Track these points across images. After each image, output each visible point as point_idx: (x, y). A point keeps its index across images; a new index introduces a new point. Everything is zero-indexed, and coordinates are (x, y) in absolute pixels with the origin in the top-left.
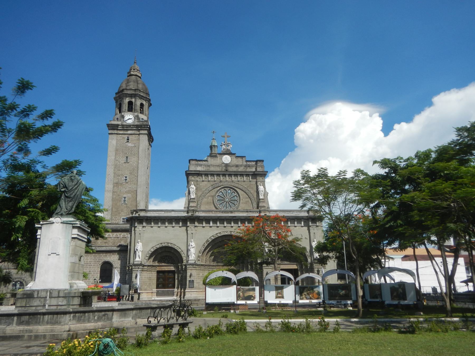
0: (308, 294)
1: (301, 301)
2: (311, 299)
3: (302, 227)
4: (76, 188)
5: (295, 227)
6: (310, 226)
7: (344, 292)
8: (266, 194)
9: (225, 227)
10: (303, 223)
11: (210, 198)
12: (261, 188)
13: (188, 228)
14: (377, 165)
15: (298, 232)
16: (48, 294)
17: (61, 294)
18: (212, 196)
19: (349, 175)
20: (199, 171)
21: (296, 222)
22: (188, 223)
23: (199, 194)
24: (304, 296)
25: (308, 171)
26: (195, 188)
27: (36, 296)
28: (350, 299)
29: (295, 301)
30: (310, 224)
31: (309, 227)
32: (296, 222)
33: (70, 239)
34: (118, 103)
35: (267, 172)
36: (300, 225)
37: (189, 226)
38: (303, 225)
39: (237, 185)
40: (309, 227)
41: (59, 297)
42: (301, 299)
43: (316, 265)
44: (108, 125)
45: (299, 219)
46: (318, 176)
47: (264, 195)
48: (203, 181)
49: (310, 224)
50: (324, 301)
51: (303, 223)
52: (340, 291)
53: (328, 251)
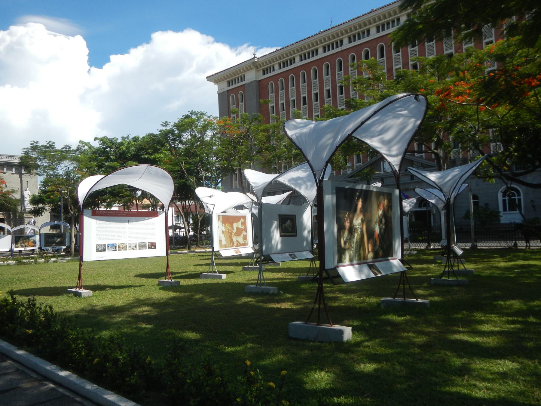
0: (24, 243)
1: (15, 249)
2: (26, 247)
3: (13, 174)
5: (4, 173)
6: (23, 174)
7: (59, 240)
10: (14, 170)
14: (97, 141)
15: (11, 180)
19: (74, 147)
21: (5, 169)
24: (19, 245)
25: (37, 142)
28: (65, 245)
29: (11, 250)
30: (23, 171)
31: (21, 175)
32: (5, 169)
36: (11, 172)
38: (14, 172)
40: (21, 175)
42: (16, 247)
43: (27, 214)
45: (9, 166)
46: (46, 147)
49: (23, 171)
50: (40, 248)
51: (14, 170)
52: (56, 239)
53: (44, 203)
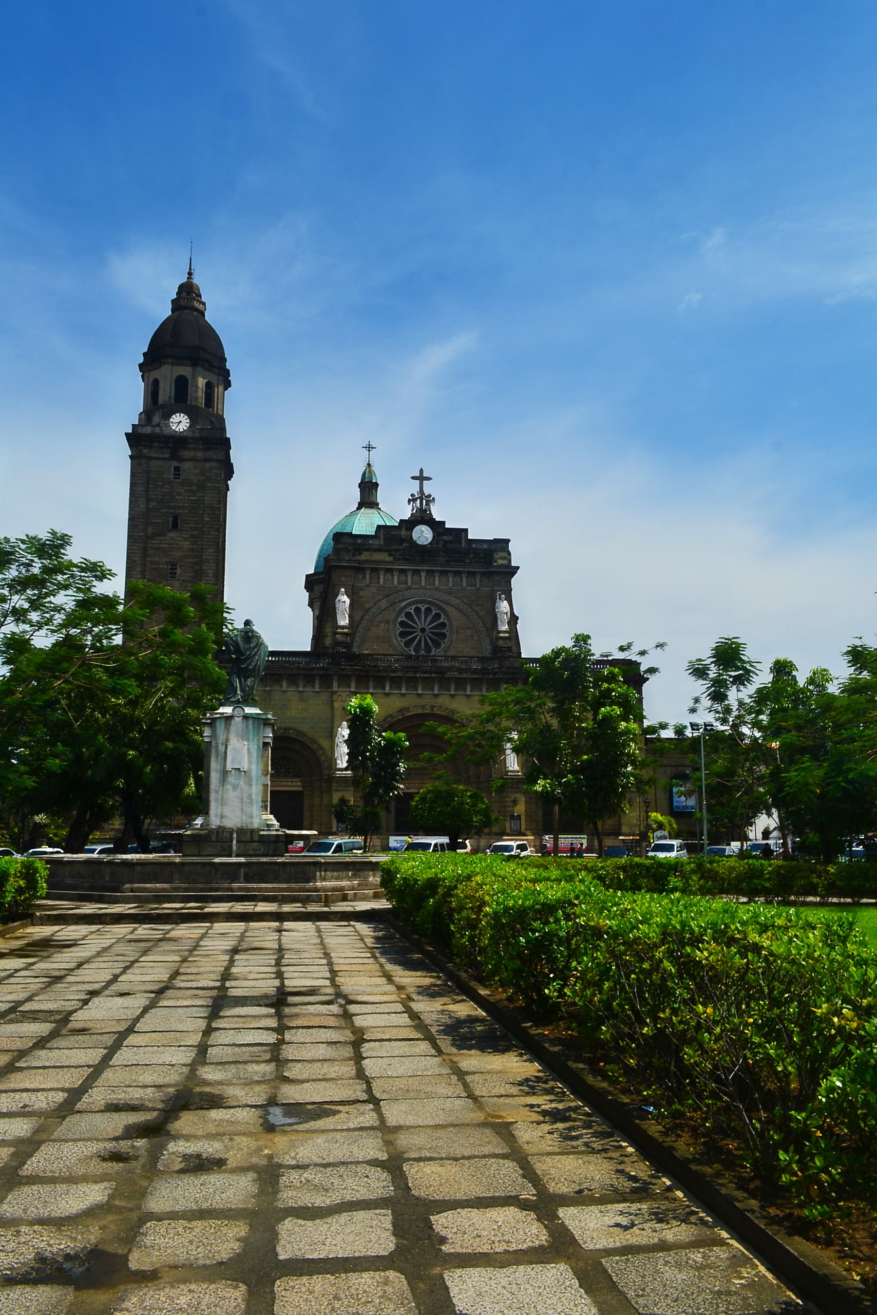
4: (255, 654)
8: (514, 620)
9: (420, 695)
11: (382, 625)
12: (504, 606)
13: (335, 697)
16: (235, 836)
17: (256, 838)
18: (388, 622)
20: (359, 562)
22: (335, 685)
23: (357, 618)
26: (348, 601)
27: (214, 838)
33: (261, 744)
34: (151, 380)
35: (518, 568)
37: (336, 692)
39: (446, 597)
41: (252, 841)
44: (126, 434)
47: (509, 623)
48: (367, 586)
